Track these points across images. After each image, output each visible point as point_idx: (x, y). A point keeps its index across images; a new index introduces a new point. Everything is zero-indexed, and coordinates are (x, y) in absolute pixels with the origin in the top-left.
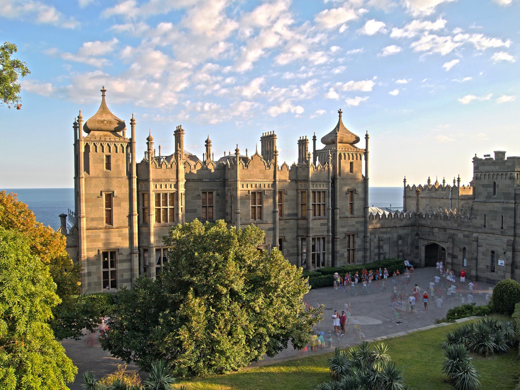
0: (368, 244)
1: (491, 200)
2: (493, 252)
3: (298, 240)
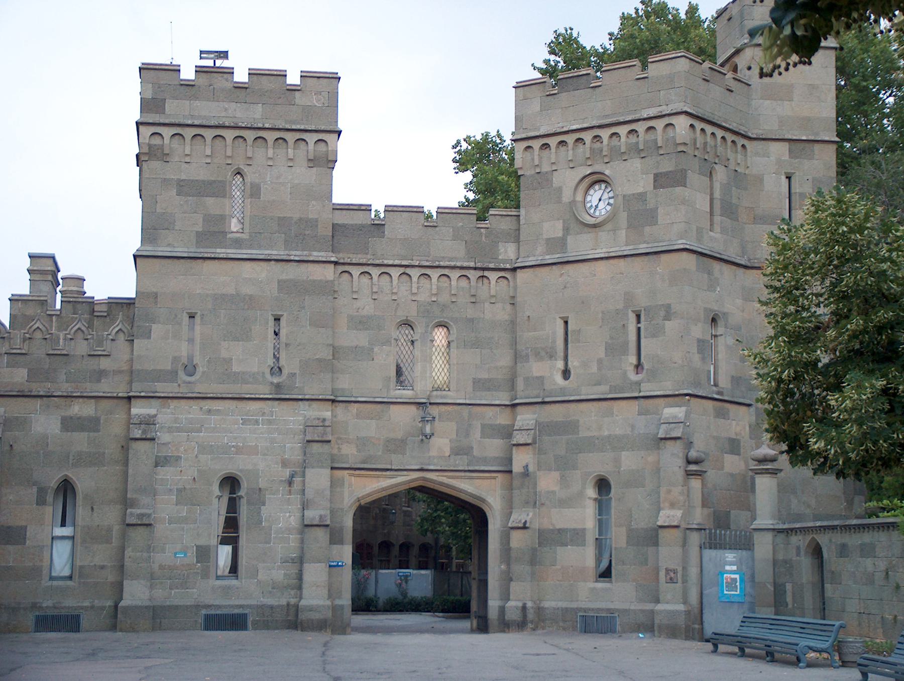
2: (231, 483)
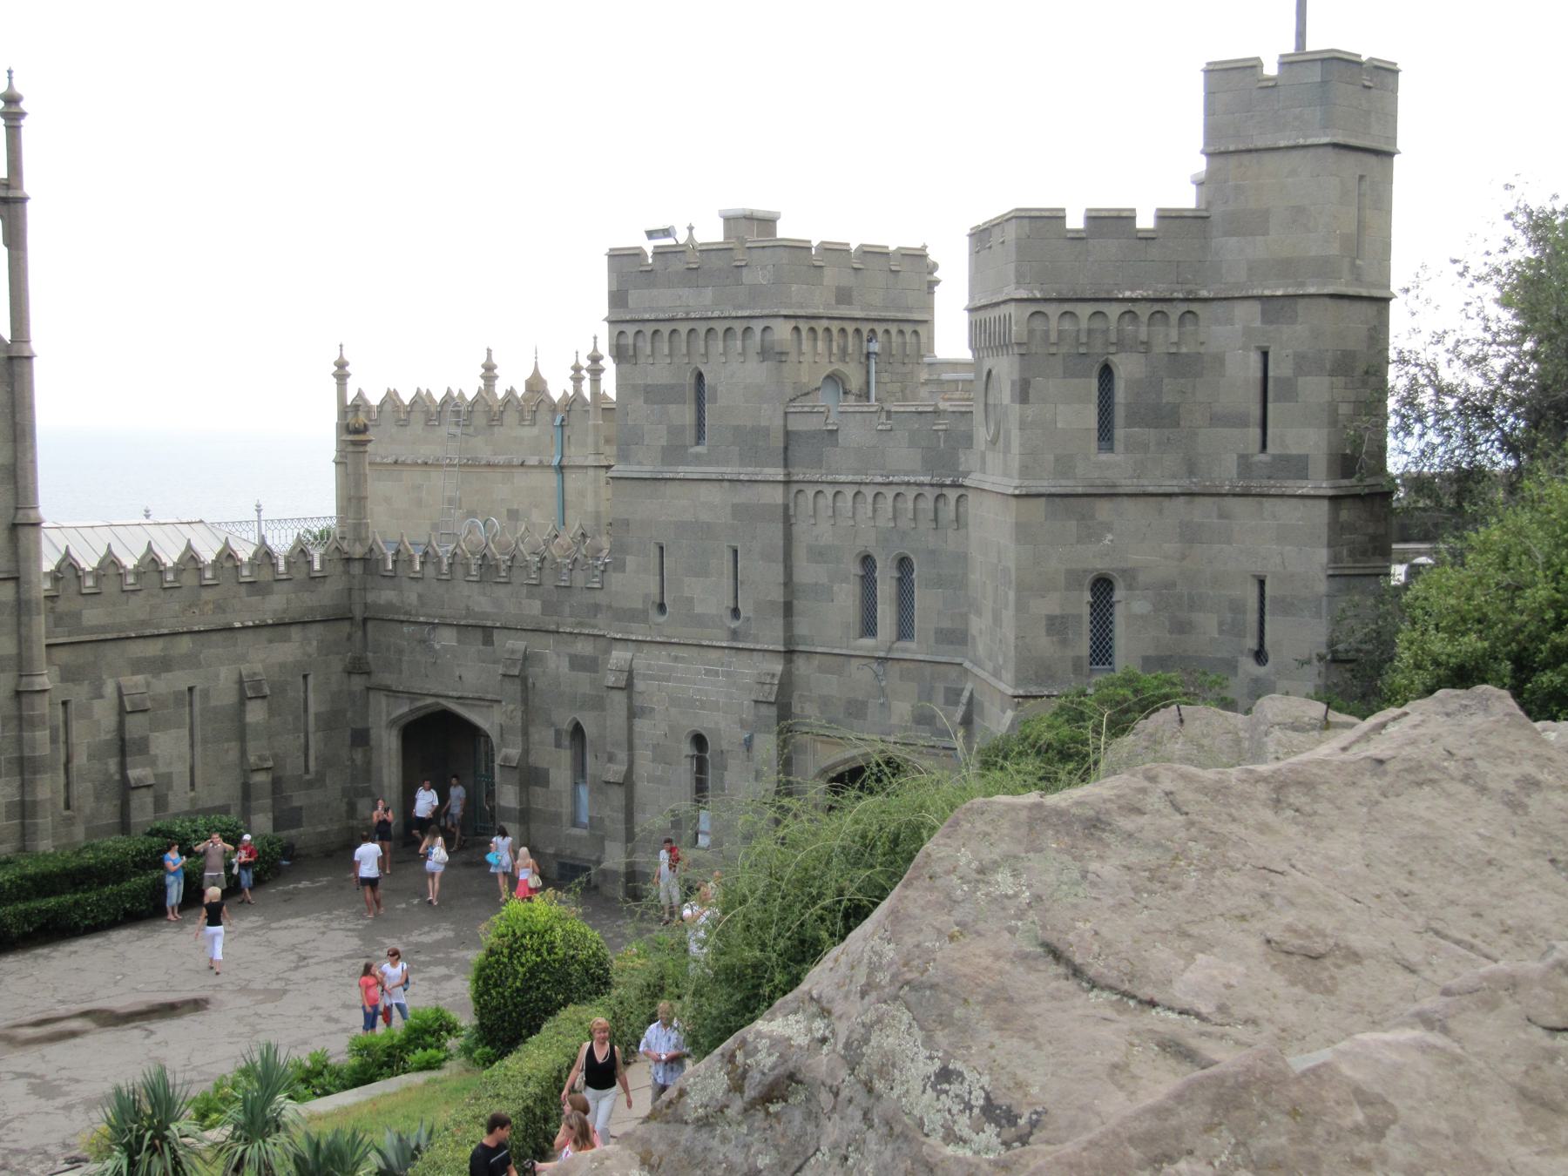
0: (43, 735)
1: (683, 471)
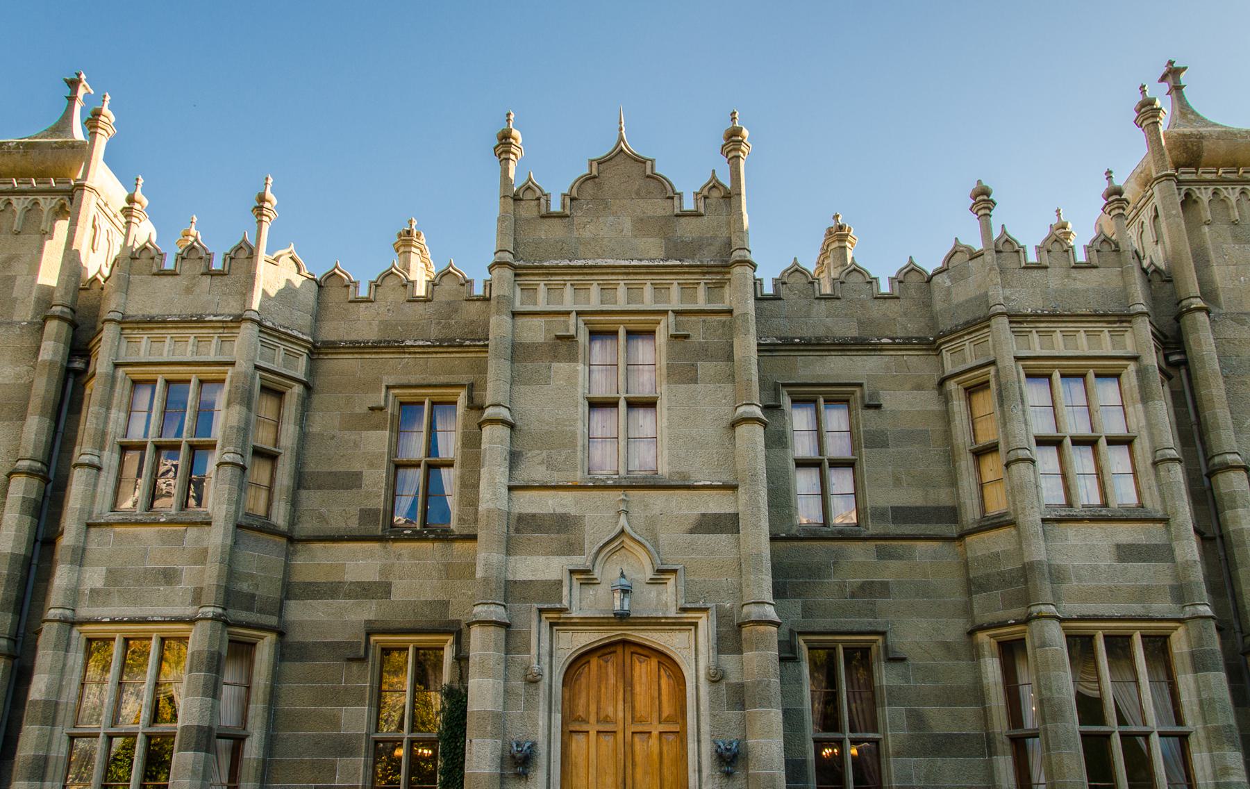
3: (975, 654)
